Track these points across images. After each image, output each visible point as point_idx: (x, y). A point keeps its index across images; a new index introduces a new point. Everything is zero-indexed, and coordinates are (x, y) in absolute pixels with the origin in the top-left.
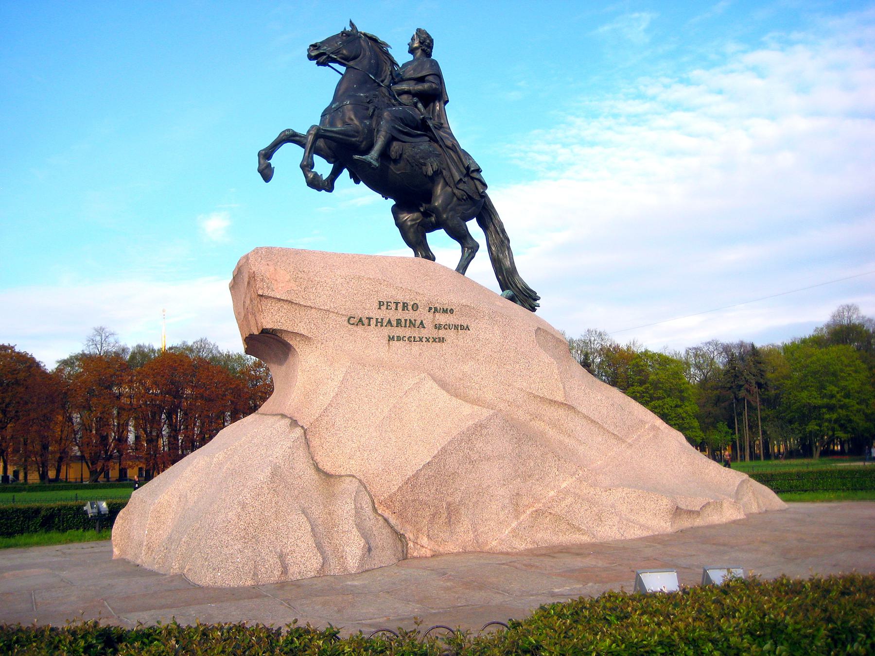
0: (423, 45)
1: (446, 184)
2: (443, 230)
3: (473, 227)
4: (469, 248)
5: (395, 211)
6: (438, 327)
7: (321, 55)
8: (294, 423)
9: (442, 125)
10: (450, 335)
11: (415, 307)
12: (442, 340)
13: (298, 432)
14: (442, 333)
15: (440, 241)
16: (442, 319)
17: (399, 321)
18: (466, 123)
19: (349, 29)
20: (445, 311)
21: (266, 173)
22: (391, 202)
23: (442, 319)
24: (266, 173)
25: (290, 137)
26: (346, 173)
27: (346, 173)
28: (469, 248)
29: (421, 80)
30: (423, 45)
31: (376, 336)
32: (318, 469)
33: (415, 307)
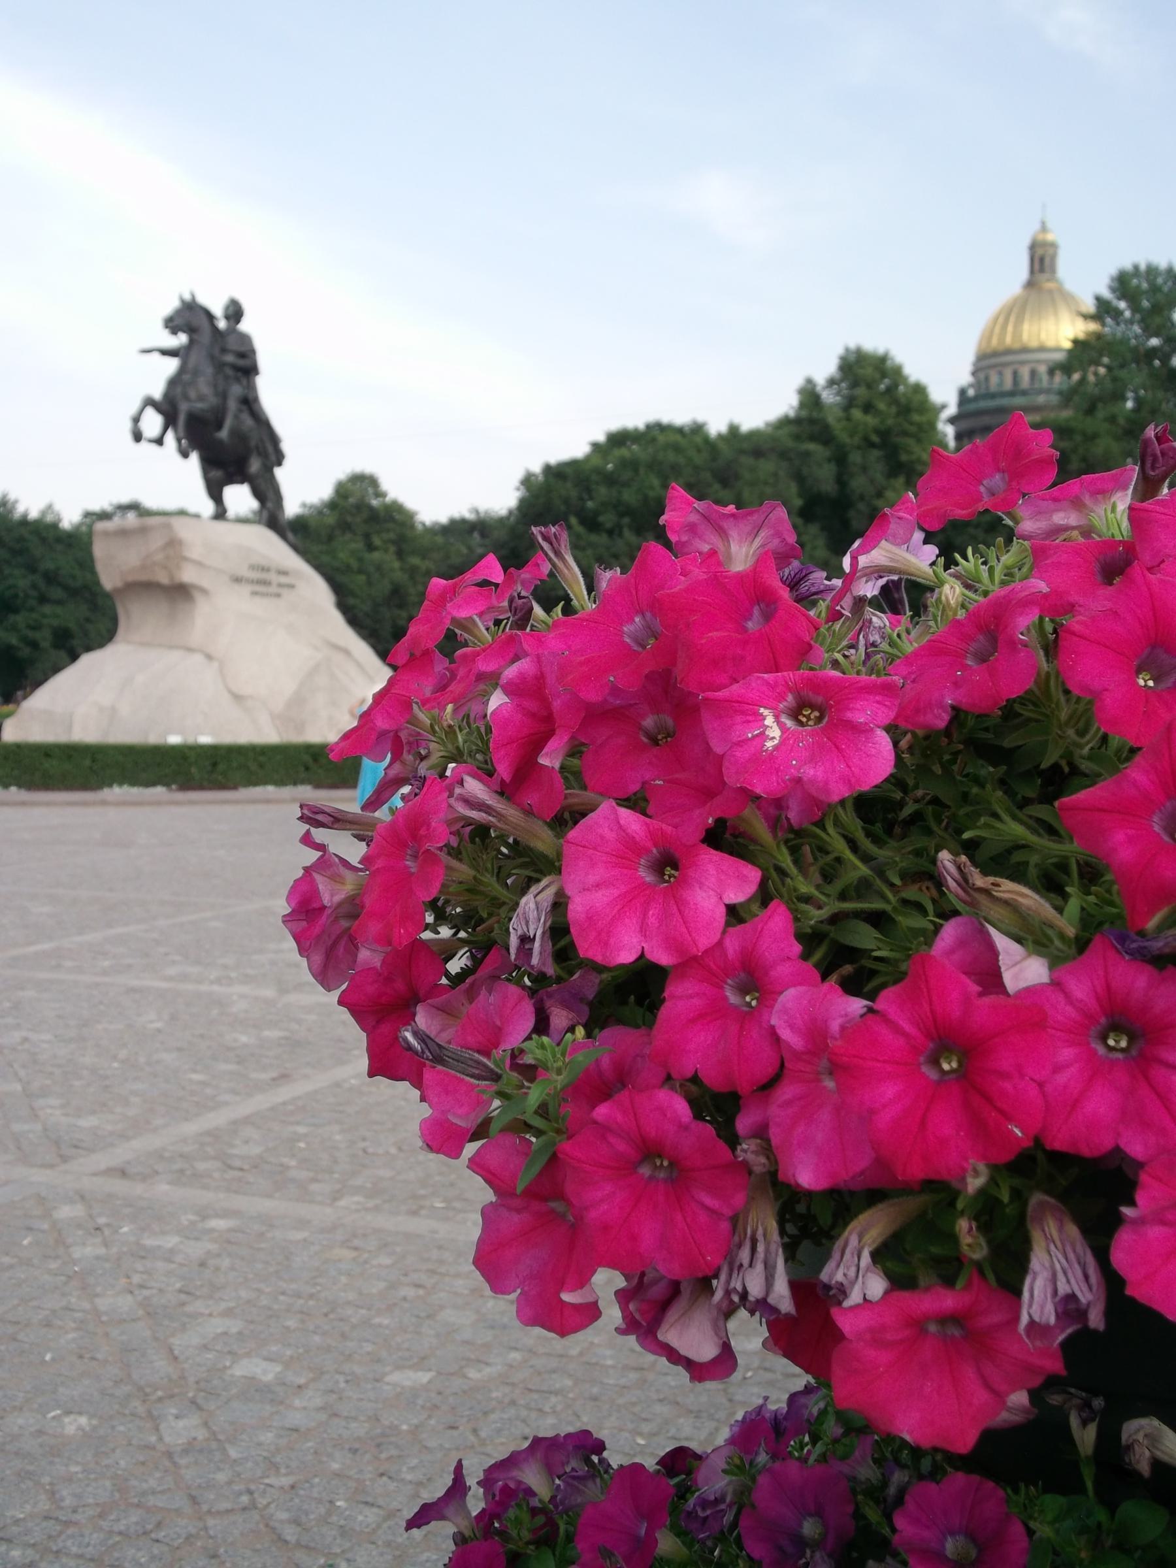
1: (259, 454)
6: (280, 585)
7: (173, 324)
8: (209, 657)
10: (285, 592)
11: (268, 570)
12: (278, 595)
13: (215, 665)
14: (280, 590)
16: (283, 580)
19: (187, 297)
21: (138, 437)
23: (283, 580)
29: (242, 355)
31: (246, 589)
32: (230, 692)
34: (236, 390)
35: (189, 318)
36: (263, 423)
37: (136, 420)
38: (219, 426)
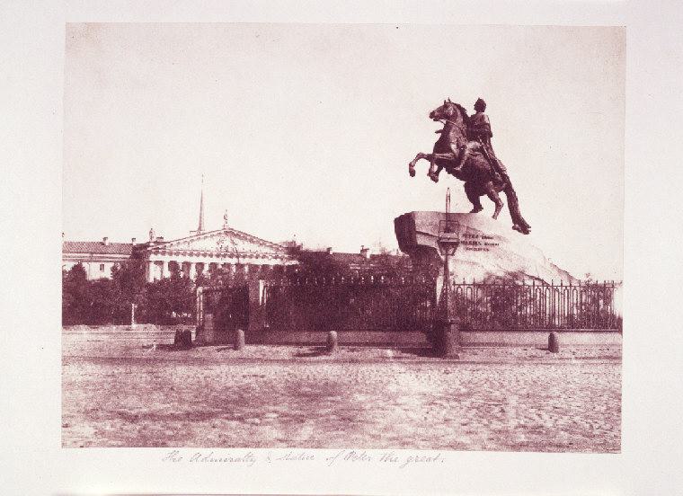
0: (480, 106)
2: (486, 197)
3: (502, 196)
4: (498, 206)
5: (466, 186)
6: (486, 244)
9: (490, 148)
15: (484, 200)
16: (488, 241)
17: (470, 242)
18: (501, 148)
20: (489, 238)
21: (412, 173)
22: (464, 182)
24: (412, 173)
25: (420, 156)
26: (444, 169)
27: (444, 169)
28: (498, 206)
30: (480, 106)
33: (477, 237)
34: (471, 145)
35: (445, 113)
36: (494, 163)
37: (411, 166)
38: (459, 164)
